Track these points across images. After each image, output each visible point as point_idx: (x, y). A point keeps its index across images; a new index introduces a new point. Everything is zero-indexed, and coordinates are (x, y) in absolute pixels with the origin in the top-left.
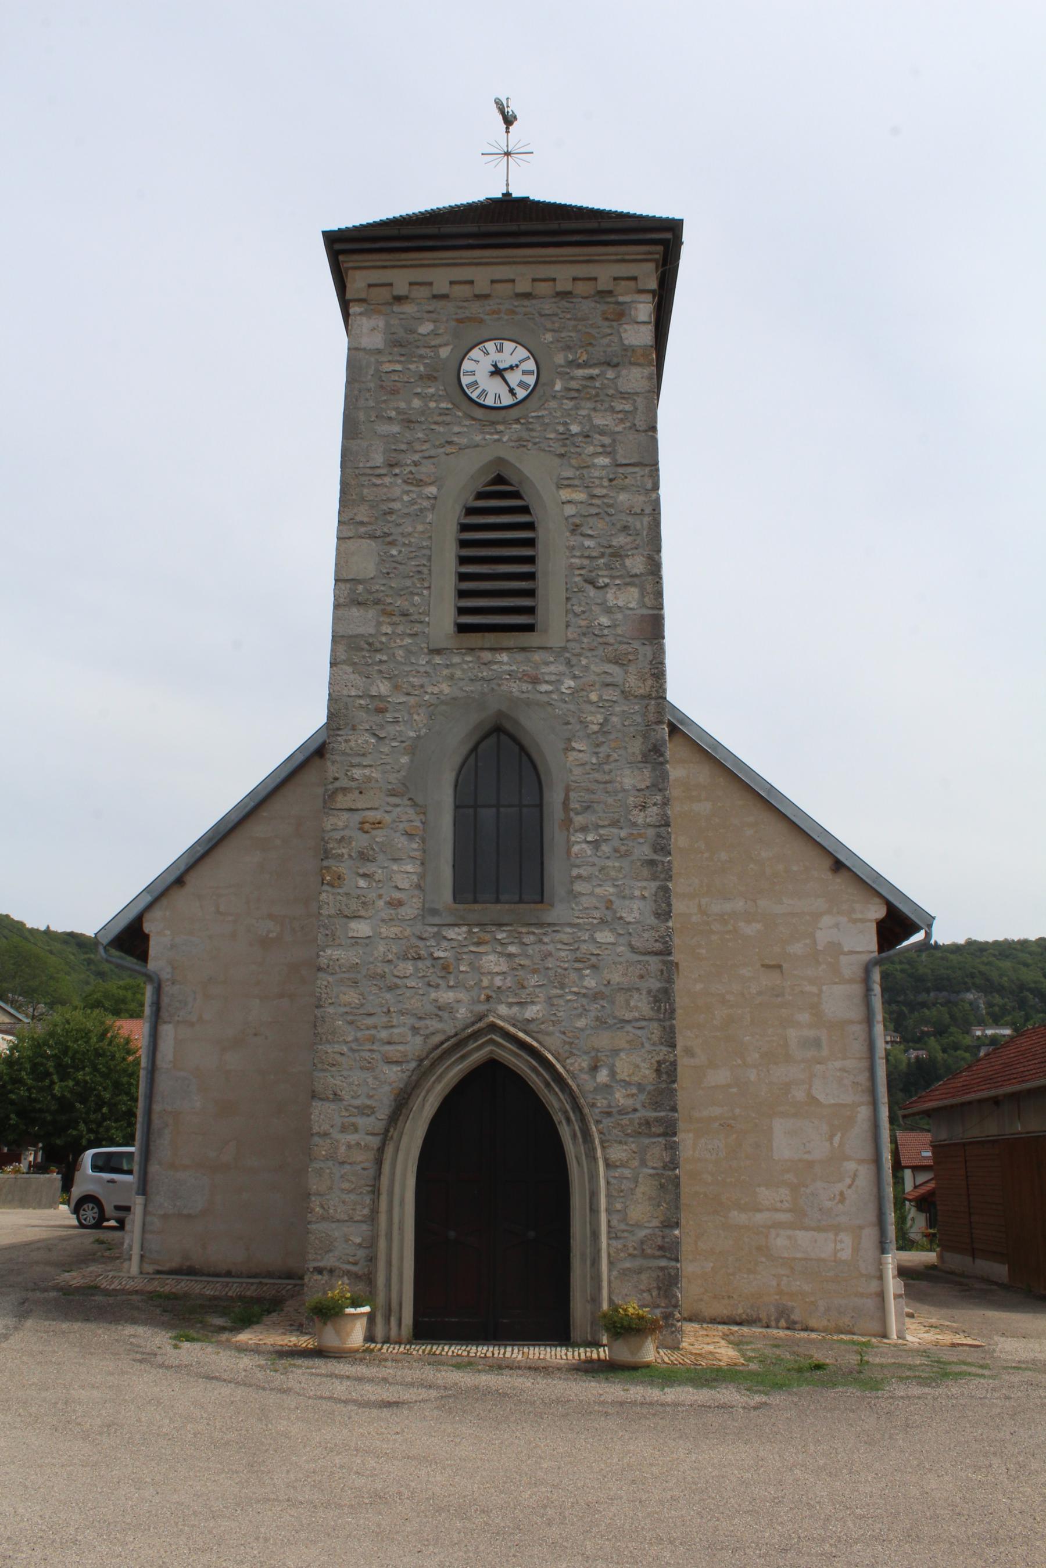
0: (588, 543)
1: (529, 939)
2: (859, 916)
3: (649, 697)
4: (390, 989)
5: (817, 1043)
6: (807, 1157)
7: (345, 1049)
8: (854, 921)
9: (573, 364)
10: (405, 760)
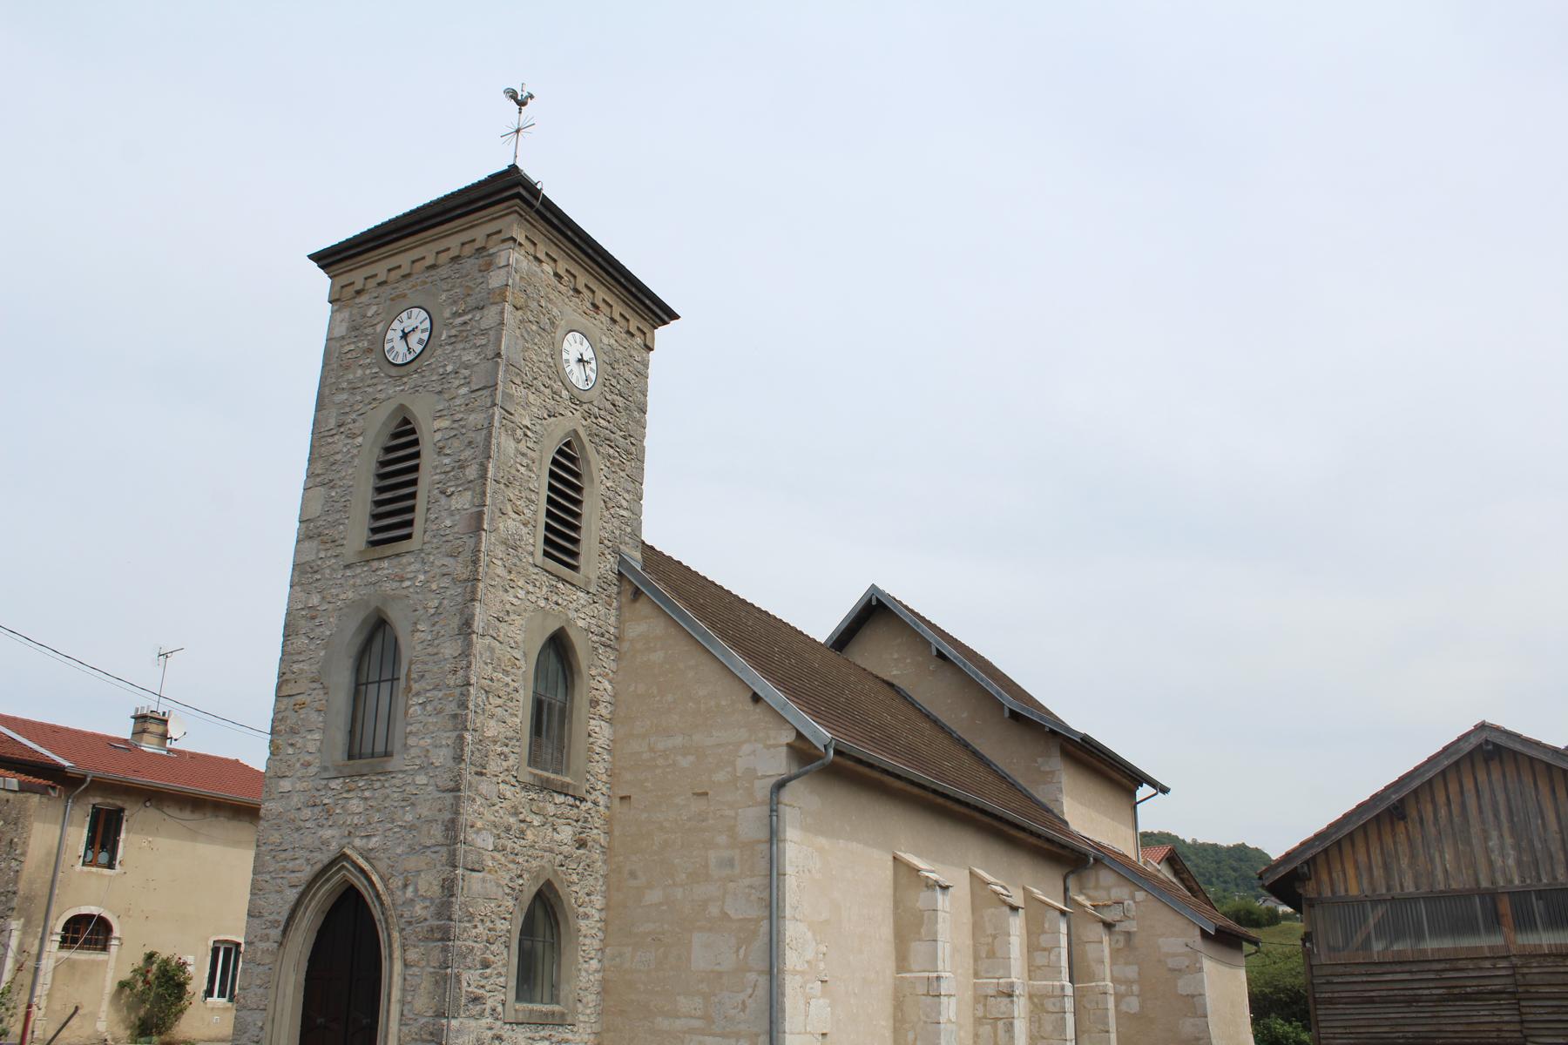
0: (447, 461)
1: (378, 785)
2: (772, 742)
3: (467, 580)
4: (298, 829)
5: (730, 863)
6: (717, 968)
7: (268, 877)
8: (768, 747)
9: (456, 315)
10: (322, 653)
